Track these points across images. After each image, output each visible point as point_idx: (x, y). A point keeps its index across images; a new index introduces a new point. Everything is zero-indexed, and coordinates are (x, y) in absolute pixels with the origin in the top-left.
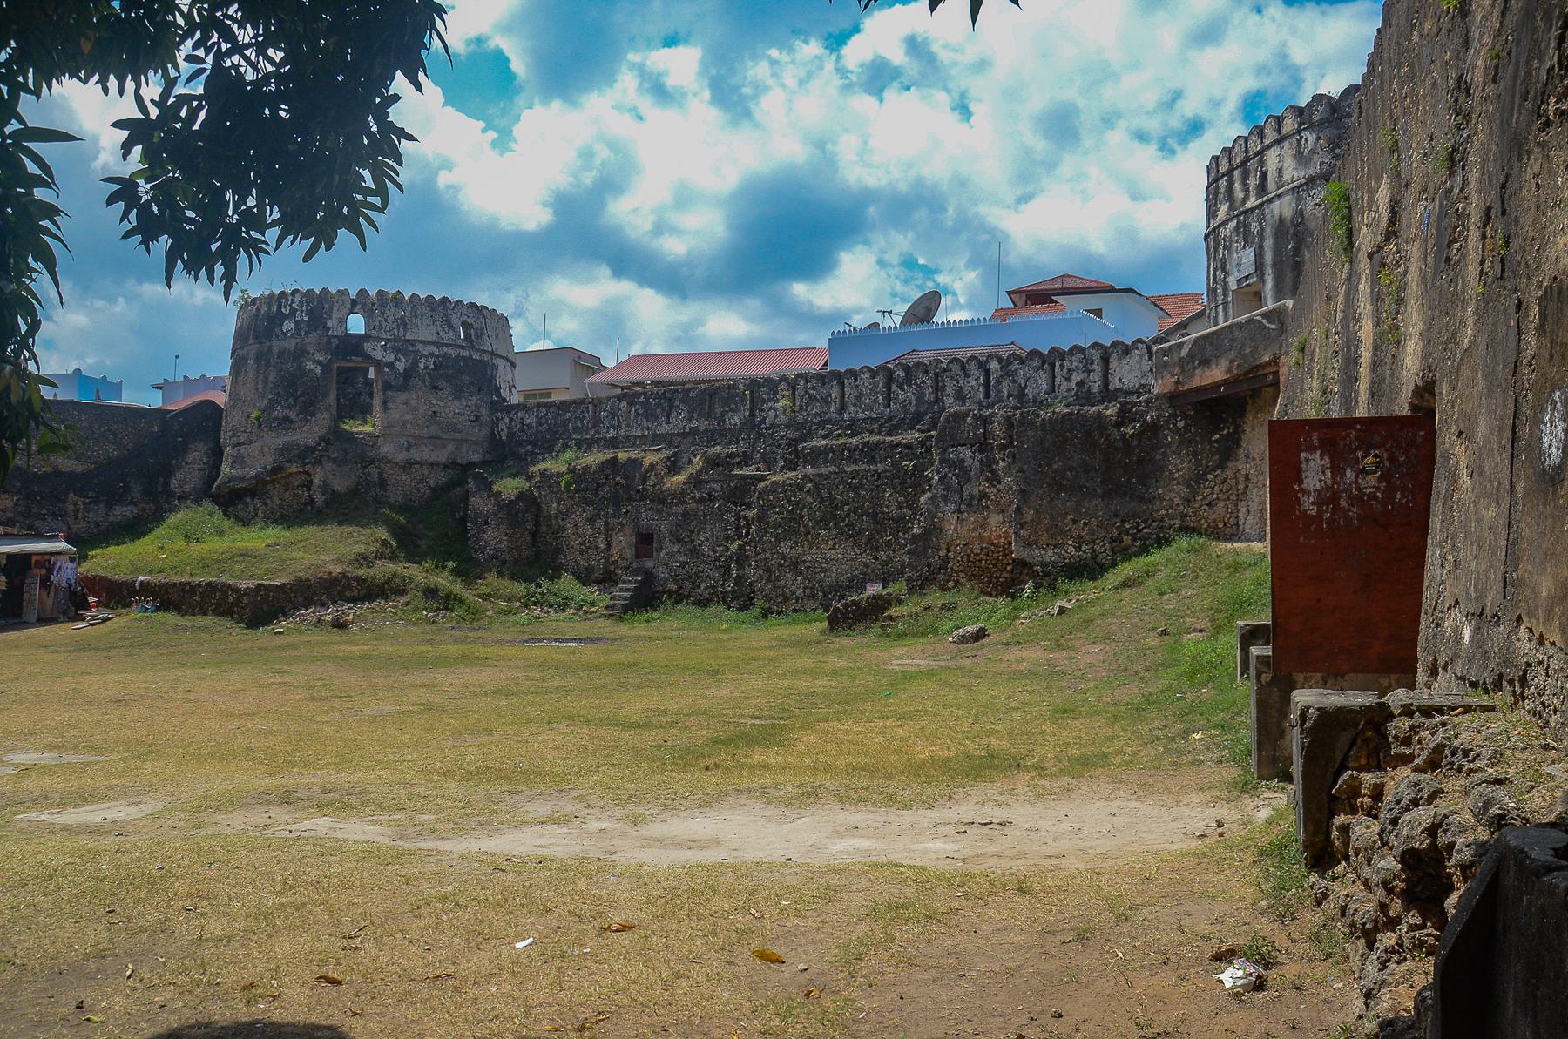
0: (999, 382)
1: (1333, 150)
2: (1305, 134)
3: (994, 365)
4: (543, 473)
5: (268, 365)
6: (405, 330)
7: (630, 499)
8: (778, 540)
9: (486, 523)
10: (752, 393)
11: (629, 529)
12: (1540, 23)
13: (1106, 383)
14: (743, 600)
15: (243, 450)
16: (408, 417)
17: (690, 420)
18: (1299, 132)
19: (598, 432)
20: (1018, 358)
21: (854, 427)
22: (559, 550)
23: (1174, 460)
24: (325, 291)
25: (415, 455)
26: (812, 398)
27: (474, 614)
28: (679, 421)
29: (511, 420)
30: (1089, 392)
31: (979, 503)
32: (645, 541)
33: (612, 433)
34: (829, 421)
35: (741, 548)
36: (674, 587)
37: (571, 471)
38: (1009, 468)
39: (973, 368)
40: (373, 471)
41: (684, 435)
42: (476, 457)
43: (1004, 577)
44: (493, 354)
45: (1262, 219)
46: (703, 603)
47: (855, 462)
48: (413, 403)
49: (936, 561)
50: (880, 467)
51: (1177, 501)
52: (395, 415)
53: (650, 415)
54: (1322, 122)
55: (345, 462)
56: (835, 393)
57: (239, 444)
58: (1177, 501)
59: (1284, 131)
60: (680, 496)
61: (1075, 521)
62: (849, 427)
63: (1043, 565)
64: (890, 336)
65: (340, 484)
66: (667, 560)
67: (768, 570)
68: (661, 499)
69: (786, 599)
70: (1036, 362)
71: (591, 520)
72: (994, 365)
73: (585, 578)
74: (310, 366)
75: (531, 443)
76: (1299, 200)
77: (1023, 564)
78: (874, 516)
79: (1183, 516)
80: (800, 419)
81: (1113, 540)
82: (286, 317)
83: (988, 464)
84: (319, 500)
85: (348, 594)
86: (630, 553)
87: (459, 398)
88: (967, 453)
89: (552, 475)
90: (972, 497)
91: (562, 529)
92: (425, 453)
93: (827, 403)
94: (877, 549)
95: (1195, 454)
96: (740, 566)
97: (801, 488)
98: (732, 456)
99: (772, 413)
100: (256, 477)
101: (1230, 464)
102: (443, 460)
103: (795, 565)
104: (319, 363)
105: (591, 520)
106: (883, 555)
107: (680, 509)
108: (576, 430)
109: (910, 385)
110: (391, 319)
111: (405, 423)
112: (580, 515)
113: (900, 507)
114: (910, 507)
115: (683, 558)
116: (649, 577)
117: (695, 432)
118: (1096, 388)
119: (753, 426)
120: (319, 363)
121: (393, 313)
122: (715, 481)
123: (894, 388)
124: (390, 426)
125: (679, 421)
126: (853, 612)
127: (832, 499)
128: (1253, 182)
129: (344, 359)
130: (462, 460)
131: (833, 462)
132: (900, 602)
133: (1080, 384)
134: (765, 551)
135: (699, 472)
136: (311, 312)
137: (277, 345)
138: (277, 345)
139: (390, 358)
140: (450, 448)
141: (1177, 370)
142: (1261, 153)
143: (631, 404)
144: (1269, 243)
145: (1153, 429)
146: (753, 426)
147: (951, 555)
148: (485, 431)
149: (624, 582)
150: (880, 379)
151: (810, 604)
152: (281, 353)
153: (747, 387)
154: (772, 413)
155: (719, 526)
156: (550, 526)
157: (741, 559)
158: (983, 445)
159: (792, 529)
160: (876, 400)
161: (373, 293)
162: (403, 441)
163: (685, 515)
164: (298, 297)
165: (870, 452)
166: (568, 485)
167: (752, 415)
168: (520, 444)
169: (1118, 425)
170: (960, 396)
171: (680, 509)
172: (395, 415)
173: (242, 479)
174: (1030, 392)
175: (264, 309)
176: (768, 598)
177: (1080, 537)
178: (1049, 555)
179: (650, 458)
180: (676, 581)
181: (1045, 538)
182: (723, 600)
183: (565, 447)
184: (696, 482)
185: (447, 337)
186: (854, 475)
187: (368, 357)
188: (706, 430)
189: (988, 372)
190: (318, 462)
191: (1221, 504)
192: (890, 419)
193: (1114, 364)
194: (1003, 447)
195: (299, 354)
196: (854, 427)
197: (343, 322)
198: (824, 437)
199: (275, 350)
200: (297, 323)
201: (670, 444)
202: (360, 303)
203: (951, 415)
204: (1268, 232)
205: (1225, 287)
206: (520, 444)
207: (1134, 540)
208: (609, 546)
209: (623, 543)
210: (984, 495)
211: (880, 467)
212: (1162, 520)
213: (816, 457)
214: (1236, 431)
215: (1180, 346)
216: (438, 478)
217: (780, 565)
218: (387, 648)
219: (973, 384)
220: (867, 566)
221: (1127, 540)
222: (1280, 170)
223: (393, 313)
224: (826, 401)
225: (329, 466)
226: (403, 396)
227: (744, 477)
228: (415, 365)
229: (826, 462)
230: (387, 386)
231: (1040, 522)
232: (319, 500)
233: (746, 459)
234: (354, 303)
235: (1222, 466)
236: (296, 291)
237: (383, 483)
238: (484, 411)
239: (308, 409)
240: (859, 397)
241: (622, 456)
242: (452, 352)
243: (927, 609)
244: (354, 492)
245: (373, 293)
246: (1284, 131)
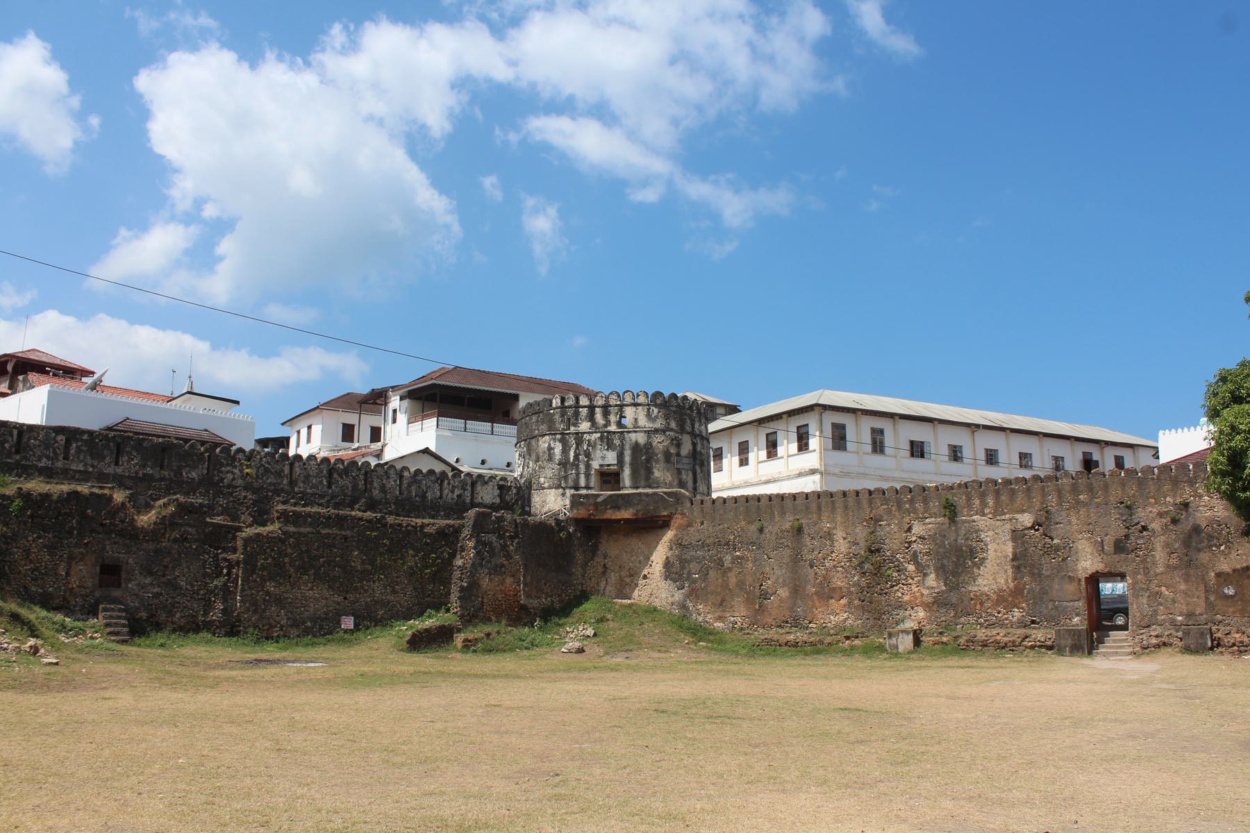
0: (409, 485)
7: (93, 531)
8: (264, 580)
13: (472, 499)
17: (144, 466)
27: (350, 641)
28: (130, 465)
31: (497, 570)
32: (111, 573)
33: (44, 463)
34: (283, 490)
35: (225, 584)
38: (516, 549)
45: (623, 440)
50: (348, 533)
62: (302, 499)
67: (255, 604)
68: (133, 534)
69: (271, 627)
70: (433, 478)
71: (51, 548)
76: (649, 437)
80: (256, 485)
88: (493, 538)
94: (347, 592)
96: (225, 601)
99: (230, 476)
106: (351, 597)
113: (363, 562)
115: (156, 590)
117: (148, 478)
118: (468, 500)
123: (335, 476)
131: (311, 524)
134: (250, 588)
135: (173, 515)
143: (68, 441)
146: (210, 483)
149: (105, 610)
151: (294, 631)
154: (230, 476)
157: (227, 593)
160: (321, 482)
163: (157, 551)
166: (22, 509)
169: (560, 531)
170: (383, 489)
171: (152, 546)
174: (429, 495)
182: (208, 626)
184: (166, 523)
189: (401, 477)
192: (332, 498)
193: (479, 488)
194: (511, 538)
205: (588, 466)
209: (83, 574)
210: (503, 566)
211: (348, 533)
215: (598, 496)
218: (376, 668)
219: (391, 483)
220: (339, 604)
222: (636, 420)
224: (279, 474)
235: (592, 559)
240: (307, 477)
241: (84, 489)
243: (488, 635)
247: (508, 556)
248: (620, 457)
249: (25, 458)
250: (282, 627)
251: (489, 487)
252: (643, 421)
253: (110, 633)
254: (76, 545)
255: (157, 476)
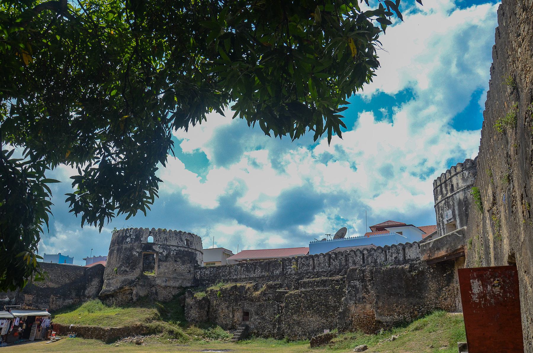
1: (474, 177)
2: (464, 172)
3: (365, 252)
4: (211, 291)
5: (121, 252)
6: (167, 241)
7: (241, 300)
8: (292, 314)
9: (191, 308)
10: (283, 263)
11: (241, 310)
12: (526, 137)
13: (405, 257)
14: (280, 336)
15: (110, 281)
16: (166, 271)
18: (462, 171)
19: (230, 276)
20: (374, 249)
21: (318, 274)
22: (216, 318)
23: (430, 283)
24: (141, 228)
25: (168, 284)
26: (303, 264)
27: (186, 340)
28: (258, 273)
29: (201, 272)
30: (399, 260)
32: (246, 315)
33: (235, 277)
34: (310, 272)
35: (280, 317)
36: (256, 331)
37: (221, 290)
38: (372, 287)
39: (358, 253)
40: (154, 289)
41: (260, 277)
42: (189, 285)
43: (373, 327)
44: (196, 250)
46: (266, 337)
47: (319, 286)
48: (168, 266)
49: (348, 321)
51: (433, 298)
52: (162, 270)
53: (248, 270)
54: (470, 168)
55: (144, 286)
56: (311, 262)
57: (109, 279)
58: (433, 298)
59: (457, 171)
60: (258, 299)
61: (397, 306)
63: (386, 322)
64: (330, 243)
65: (142, 293)
66: (254, 321)
67: (289, 325)
69: (296, 335)
70: (380, 251)
71: (228, 307)
72: (365, 252)
73: (225, 328)
74: (135, 253)
75: (207, 280)
76: (465, 193)
77: (379, 322)
78: (326, 305)
79: (436, 303)
80: (299, 272)
81: (411, 313)
82: (128, 237)
83: (365, 287)
84: (135, 299)
85: (142, 332)
86: (241, 319)
87: (184, 265)
88: (357, 283)
89: (214, 291)
90: (360, 298)
91: (217, 310)
92: (171, 283)
93: (309, 266)
94: (327, 318)
95: (438, 281)
96: (279, 324)
97: (300, 296)
98: (276, 285)
99: (290, 270)
100: (114, 290)
101: (451, 284)
102: (177, 285)
103: (298, 323)
104: (138, 252)
105: (228, 307)
107: (258, 303)
108: (223, 276)
109: (337, 260)
110: (162, 238)
111: (165, 273)
112: (224, 305)
113: (335, 302)
114: (338, 302)
115: (259, 321)
116: (247, 327)
117: (263, 276)
118: (401, 259)
119: (283, 274)
120: (138, 252)
121: (163, 236)
122: (270, 293)
123: (331, 260)
124: (160, 274)
125: (258, 273)
126: (319, 340)
127: (311, 299)
128: (449, 188)
129: (146, 251)
130: (184, 286)
132: (336, 336)
133: (396, 258)
134: (288, 318)
135: (265, 290)
136: (136, 235)
137: (124, 246)
138: (124, 246)
139: (161, 251)
140: (180, 281)
141: (429, 252)
142: (450, 178)
143: (241, 267)
144: (456, 208)
145: (422, 273)
146: (283, 274)
147: (353, 319)
148: (192, 276)
150: (327, 258)
151: (304, 337)
152: (125, 249)
153: (281, 261)
154: (290, 270)
155: (272, 309)
156: (213, 309)
157: (279, 321)
158: (363, 280)
159: (297, 310)
160: (325, 265)
161: (157, 229)
162: (164, 279)
163: (260, 305)
164: (132, 230)
165: (324, 283)
166: (220, 295)
167: (283, 270)
168: (204, 280)
169: (410, 272)
170: (354, 263)
171: (258, 303)
172: (162, 270)
173: (109, 291)
174: (378, 261)
175: (121, 234)
176: (289, 335)
177: (399, 312)
178: (388, 319)
179: (248, 285)
180: (257, 329)
181: (386, 313)
182: (273, 336)
183: (219, 282)
184: (264, 294)
185: (181, 244)
186: (319, 291)
187: (154, 250)
188: (267, 276)
189: (363, 255)
190: (135, 286)
191: (449, 299)
192: (330, 271)
193: (407, 250)
194: (370, 280)
195: (131, 249)
196: (318, 274)
197: (146, 239)
198: (308, 278)
199: (124, 248)
200: (131, 239)
201: (255, 281)
202: (152, 232)
203: (351, 270)
204: (456, 204)
205: (443, 223)
206: (204, 280)
207: (419, 312)
208: (233, 316)
209: (238, 315)
210: (364, 298)
211: (327, 288)
212: (428, 305)
213: (305, 285)
214: (452, 273)
215: (429, 243)
216: (175, 292)
217: (293, 323)
219: (359, 259)
220: (324, 324)
221: (416, 312)
222: (457, 184)
223: (163, 236)
224: (308, 265)
225: (138, 287)
226: (165, 264)
227: (280, 292)
228: (169, 253)
229: (309, 287)
230: (160, 260)
231: (384, 307)
232: (135, 299)
233: (281, 286)
234: (150, 232)
235: (448, 285)
236: (132, 228)
237: (156, 293)
238: (192, 269)
239: (133, 268)
240: (320, 264)
241: (238, 285)
242: (182, 249)
243: (346, 339)
244: (146, 296)
245: (157, 229)
246: (457, 171)
247: (367, 292)
248: (454, 212)
249: (230, 276)
250: (299, 335)
251: (413, 249)
252: (462, 184)
253: (232, 338)
254: (235, 306)
255: (266, 275)
